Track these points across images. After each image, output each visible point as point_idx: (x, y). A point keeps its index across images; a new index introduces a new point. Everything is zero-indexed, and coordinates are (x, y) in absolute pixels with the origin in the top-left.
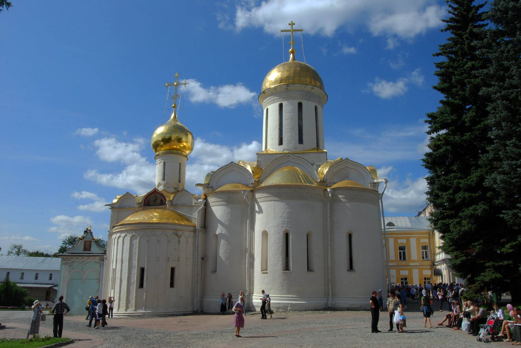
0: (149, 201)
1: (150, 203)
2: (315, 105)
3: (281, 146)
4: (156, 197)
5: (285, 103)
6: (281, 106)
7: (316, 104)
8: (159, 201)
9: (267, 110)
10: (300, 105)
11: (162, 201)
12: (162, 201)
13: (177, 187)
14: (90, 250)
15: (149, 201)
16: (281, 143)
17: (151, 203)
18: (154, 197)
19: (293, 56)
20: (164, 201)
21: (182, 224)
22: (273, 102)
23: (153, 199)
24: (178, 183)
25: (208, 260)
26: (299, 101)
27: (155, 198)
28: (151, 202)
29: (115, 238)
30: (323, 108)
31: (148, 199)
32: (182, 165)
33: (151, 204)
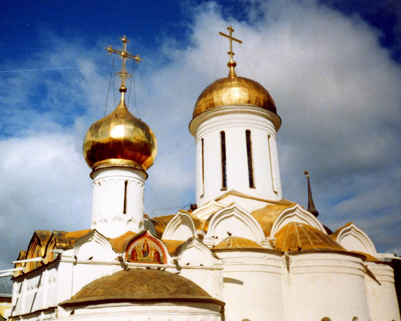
1: (136, 255)
4: (148, 245)
6: (248, 133)
8: (152, 254)
9: (223, 134)
11: (157, 253)
12: (157, 253)
15: (134, 251)
16: (252, 185)
17: (138, 256)
18: (144, 246)
20: (161, 255)
23: (142, 249)
27: (146, 246)
28: (138, 254)
31: (132, 247)
33: (139, 258)
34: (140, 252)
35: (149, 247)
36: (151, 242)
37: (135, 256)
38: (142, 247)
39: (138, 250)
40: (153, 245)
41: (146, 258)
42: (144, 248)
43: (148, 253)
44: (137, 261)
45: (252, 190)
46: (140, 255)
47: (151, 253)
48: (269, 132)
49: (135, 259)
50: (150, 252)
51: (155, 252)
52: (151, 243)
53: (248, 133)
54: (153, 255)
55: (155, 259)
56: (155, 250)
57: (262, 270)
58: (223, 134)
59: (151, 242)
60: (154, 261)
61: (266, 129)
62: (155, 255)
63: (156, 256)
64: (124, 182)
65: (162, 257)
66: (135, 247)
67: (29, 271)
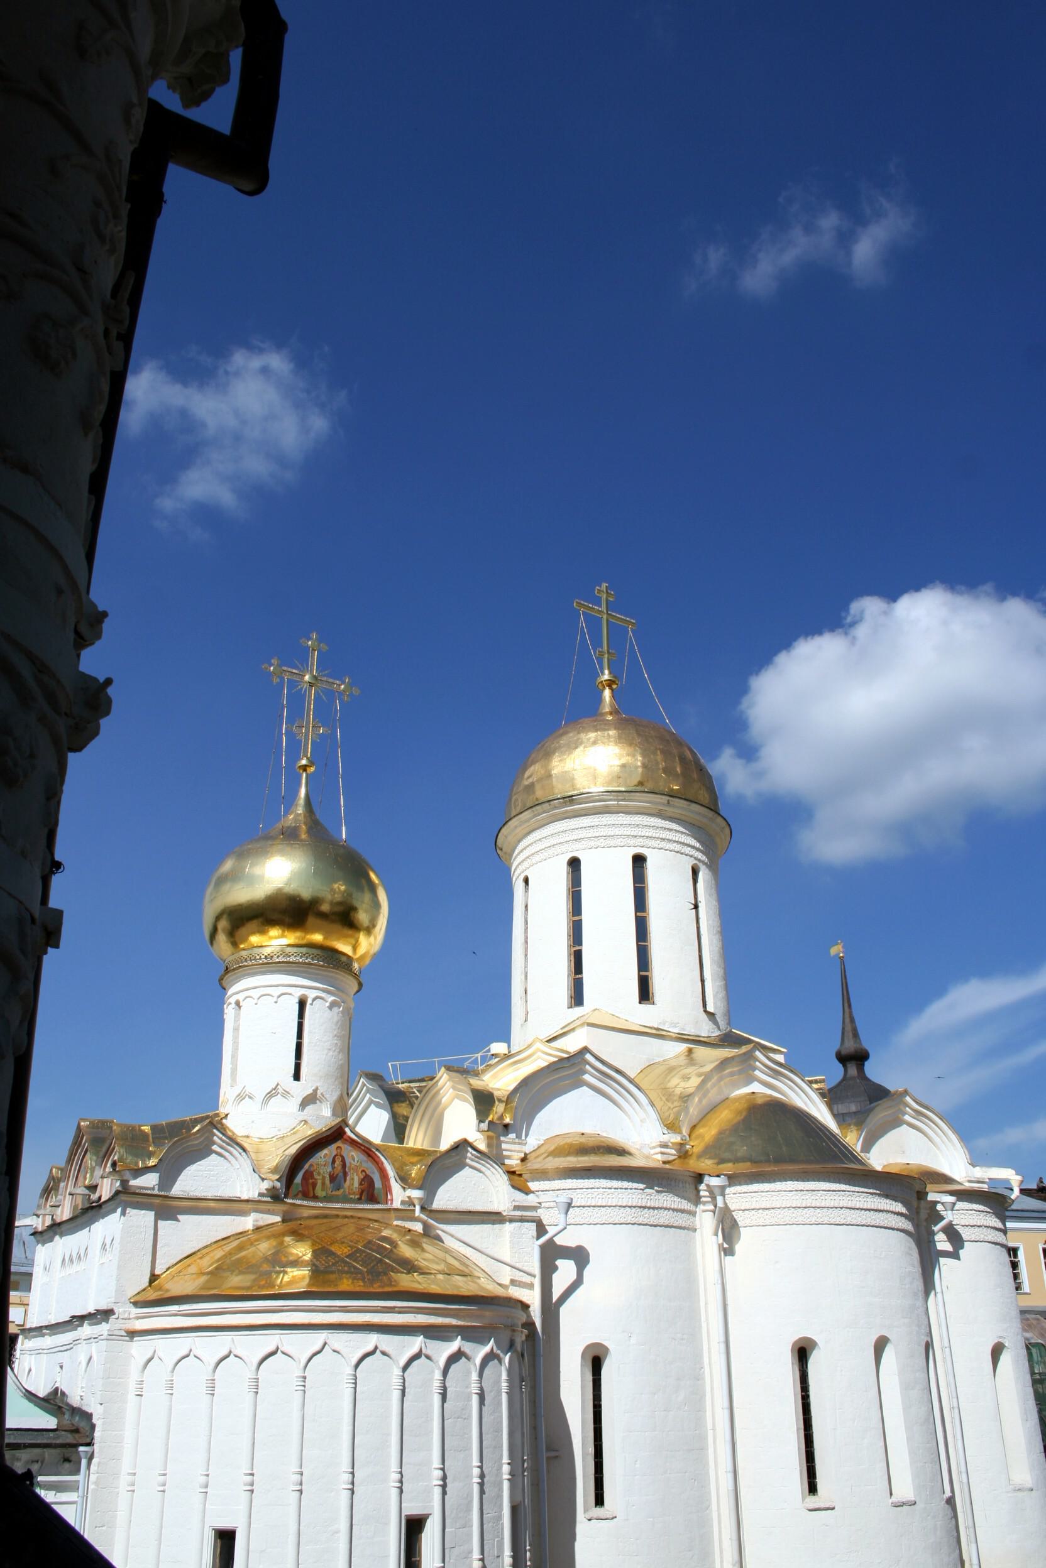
0: (309, 1175)
1: (314, 1185)
6: (639, 861)
8: (354, 1182)
9: (574, 864)
11: (367, 1181)
12: (367, 1181)
16: (645, 993)
18: (334, 1162)
20: (378, 1184)
23: (329, 1169)
25: (557, 1457)
27: (338, 1162)
28: (319, 1183)
33: (319, 1192)
34: (324, 1178)
35: (348, 1164)
36: (353, 1153)
39: (319, 1174)
40: (356, 1159)
41: (337, 1193)
42: (333, 1168)
44: (315, 1198)
45: (645, 1007)
46: (323, 1184)
47: (353, 1179)
48: (696, 859)
49: (312, 1195)
50: (348, 1178)
51: (362, 1177)
52: (352, 1156)
53: (639, 861)
54: (356, 1184)
55: (361, 1194)
56: (363, 1171)
57: (641, 1220)
58: (574, 864)
59: (353, 1153)
60: (360, 1199)
61: (687, 850)
62: (361, 1184)
63: (366, 1185)
64: (297, 1001)
65: (379, 1189)
67: (68, 1218)
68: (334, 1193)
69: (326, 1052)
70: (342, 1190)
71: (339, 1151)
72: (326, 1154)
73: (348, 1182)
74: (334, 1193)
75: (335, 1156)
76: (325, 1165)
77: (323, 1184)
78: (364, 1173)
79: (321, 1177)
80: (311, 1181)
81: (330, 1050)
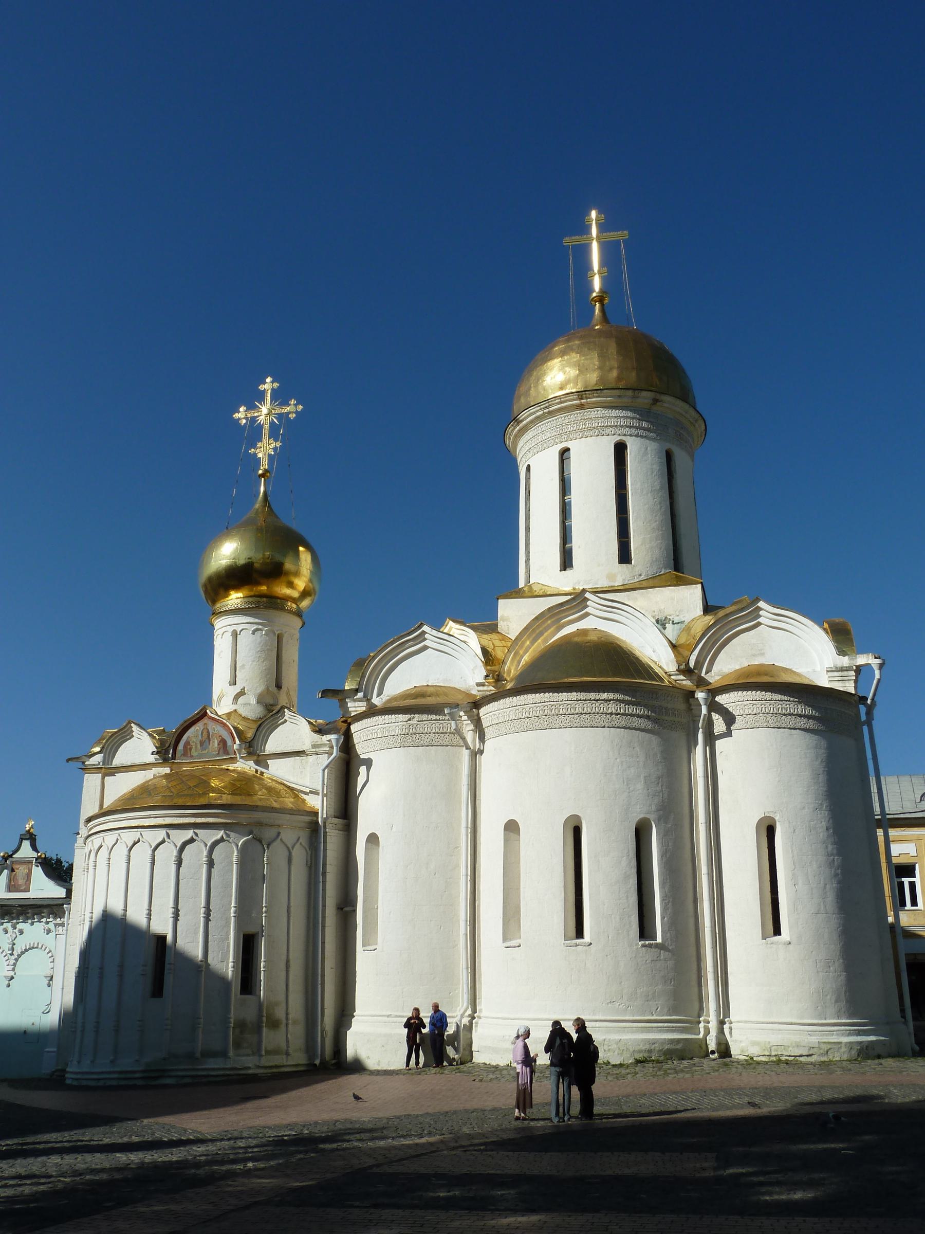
0: (187, 743)
1: (191, 749)
2: (667, 448)
3: (568, 572)
4: (208, 732)
5: (576, 447)
6: (564, 454)
7: (668, 446)
10: (620, 450)
13: (272, 702)
14: (27, 890)
16: (566, 562)
19: (603, 310)
21: (276, 809)
22: (543, 446)
24: (274, 689)
26: (617, 438)
27: (205, 733)
28: (194, 747)
29: (91, 851)
30: (692, 456)
32: (284, 640)
33: (194, 753)
35: (211, 734)
37: (189, 751)
38: (200, 736)
39: (193, 742)
40: (216, 730)
42: (202, 737)
43: (209, 744)
44: (192, 757)
46: (196, 747)
47: (214, 742)
50: (211, 742)
51: (219, 740)
53: (564, 454)
54: (216, 745)
56: (220, 736)
60: (219, 754)
62: (219, 745)
63: (221, 745)
66: (189, 737)
68: (203, 752)
69: (250, 663)
70: (207, 751)
71: (205, 726)
72: (197, 729)
73: (211, 745)
74: (203, 752)
75: (203, 729)
76: (197, 736)
77: (196, 747)
78: (220, 738)
79: (194, 744)
80: (189, 747)
81: (254, 661)
